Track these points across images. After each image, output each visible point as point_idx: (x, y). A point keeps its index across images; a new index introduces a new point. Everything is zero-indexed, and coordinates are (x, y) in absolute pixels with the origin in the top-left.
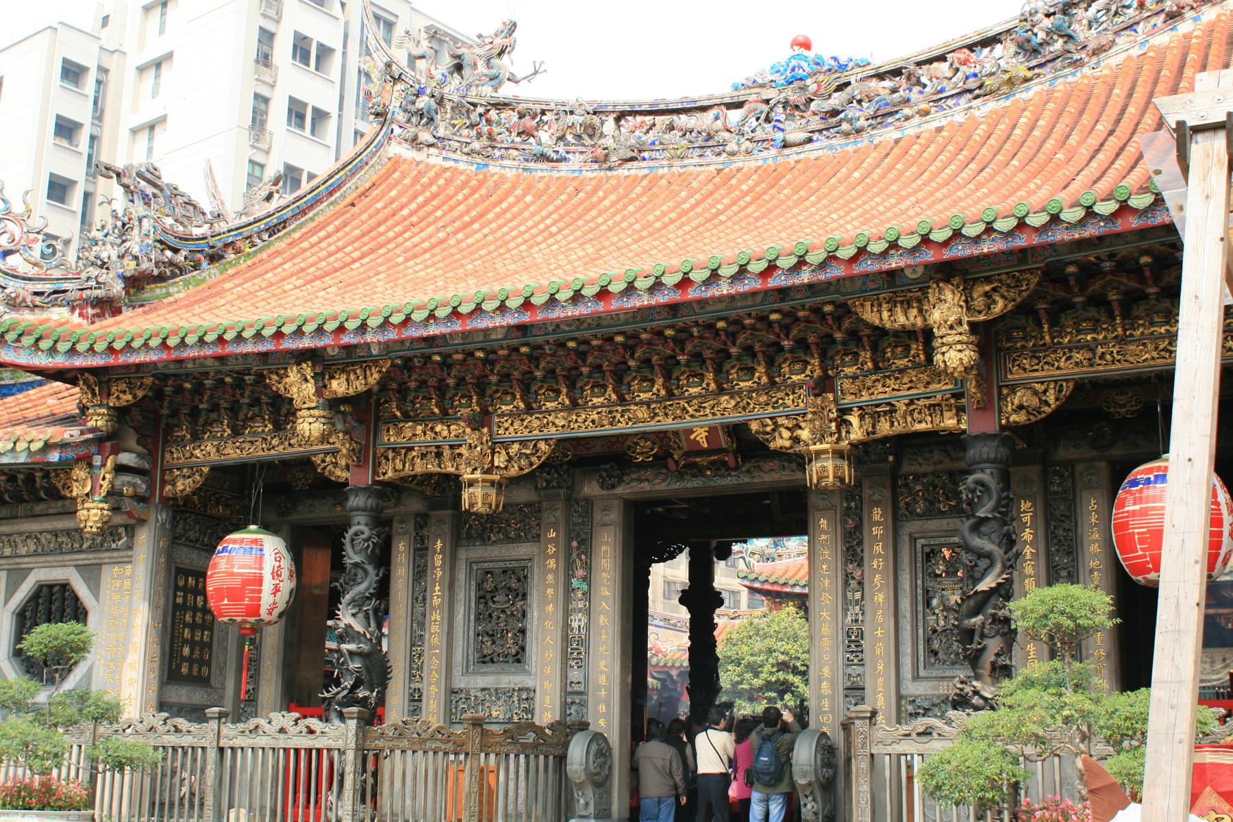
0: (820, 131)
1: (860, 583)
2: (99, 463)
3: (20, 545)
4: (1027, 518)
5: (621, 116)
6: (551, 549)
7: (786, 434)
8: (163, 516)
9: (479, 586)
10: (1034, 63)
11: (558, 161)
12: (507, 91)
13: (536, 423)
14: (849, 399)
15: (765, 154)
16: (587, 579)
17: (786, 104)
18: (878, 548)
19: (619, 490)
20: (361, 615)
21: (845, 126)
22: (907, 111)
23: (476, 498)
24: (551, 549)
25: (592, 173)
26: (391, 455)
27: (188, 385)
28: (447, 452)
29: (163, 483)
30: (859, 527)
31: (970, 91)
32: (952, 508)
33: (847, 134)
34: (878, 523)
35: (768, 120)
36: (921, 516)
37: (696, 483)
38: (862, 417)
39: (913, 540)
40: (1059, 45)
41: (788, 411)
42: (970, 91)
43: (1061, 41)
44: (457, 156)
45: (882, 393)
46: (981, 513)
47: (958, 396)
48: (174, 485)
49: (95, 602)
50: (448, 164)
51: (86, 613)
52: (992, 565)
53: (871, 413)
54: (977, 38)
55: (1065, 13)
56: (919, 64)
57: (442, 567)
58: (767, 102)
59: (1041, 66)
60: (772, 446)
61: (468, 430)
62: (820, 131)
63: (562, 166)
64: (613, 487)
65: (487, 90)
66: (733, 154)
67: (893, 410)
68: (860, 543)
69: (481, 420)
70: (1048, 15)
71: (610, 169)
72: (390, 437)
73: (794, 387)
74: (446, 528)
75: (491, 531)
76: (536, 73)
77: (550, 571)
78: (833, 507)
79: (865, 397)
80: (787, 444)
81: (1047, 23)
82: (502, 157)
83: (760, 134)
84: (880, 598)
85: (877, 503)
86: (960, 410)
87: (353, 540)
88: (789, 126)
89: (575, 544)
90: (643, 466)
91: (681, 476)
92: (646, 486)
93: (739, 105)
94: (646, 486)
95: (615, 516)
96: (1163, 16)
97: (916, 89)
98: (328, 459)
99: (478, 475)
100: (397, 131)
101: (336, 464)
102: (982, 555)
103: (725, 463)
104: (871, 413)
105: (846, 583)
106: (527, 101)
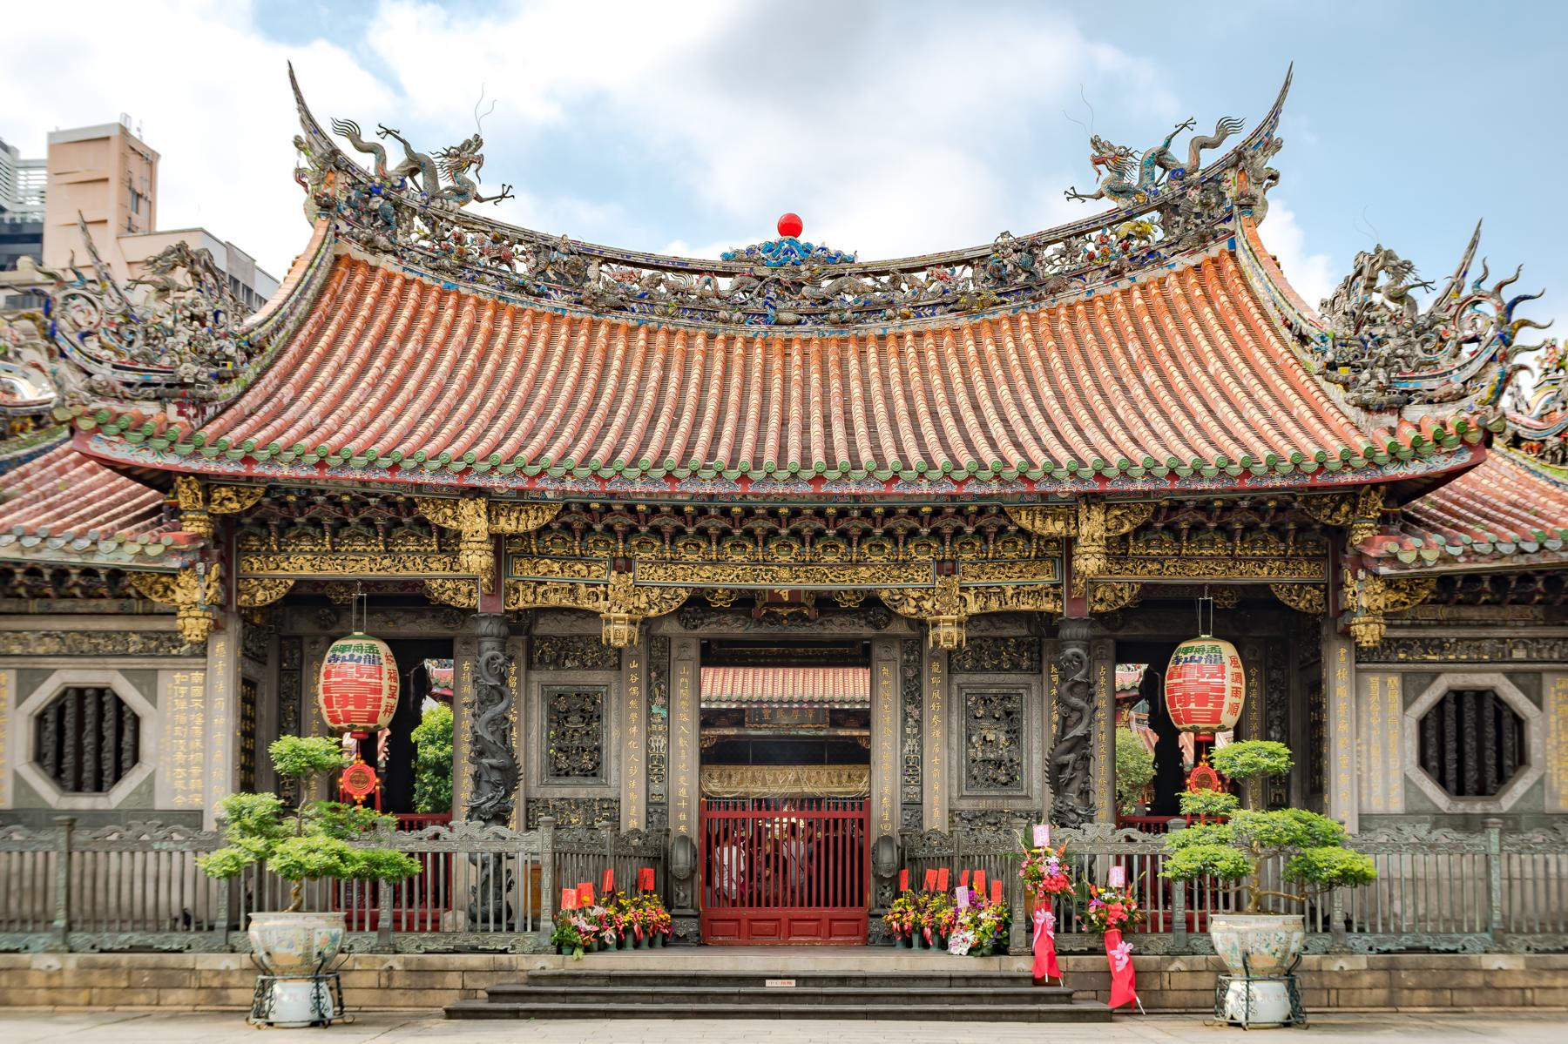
0: (809, 315)
1: (919, 723)
2: (202, 572)
3: (33, 644)
4: (1056, 678)
5: (607, 261)
6: (634, 679)
7: (913, 603)
8: (239, 626)
9: (551, 708)
10: (1001, 290)
11: (540, 295)
12: (472, 208)
13: (680, 573)
14: (969, 581)
15: (755, 327)
16: (667, 706)
17: (777, 281)
18: (936, 695)
19: (698, 631)
20: (498, 734)
21: (833, 316)
22: (890, 312)
23: (619, 633)
24: (634, 679)
25: (583, 314)
26: (521, 587)
27: (292, 498)
28: (582, 589)
29: (239, 591)
30: (918, 676)
31: (945, 304)
32: (994, 666)
33: (834, 323)
34: (936, 675)
35: (759, 294)
36: (969, 671)
37: (775, 630)
38: (977, 596)
39: (960, 688)
40: (1022, 278)
41: (917, 585)
42: (945, 304)
43: (1024, 276)
44: (421, 269)
45: (996, 579)
46: (1077, 677)
47: (1055, 586)
48: (253, 596)
49: (150, 707)
50: (409, 276)
51: (136, 720)
52: (1081, 719)
53: (984, 593)
54: (954, 258)
55: (1030, 252)
56: (903, 271)
57: (518, 688)
58: (761, 279)
59: (1006, 294)
60: (899, 611)
61: (614, 573)
62: (809, 315)
63: (544, 301)
64: (696, 627)
65: (452, 204)
66: (724, 321)
67: (1003, 591)
68: (919, 689)
69: (624, 565)
70: (1016, 251)
71: (597, 314)
72: (525, 570)
73: (920, 564)
74: (521, 654)
75: (566, 657)
76: (503, 196)
77: (634, 697)
78: (894, 660)
79: (984, 581)
80: (913, 611)
81: (1015, 257)
82: (473, 279)
83: (751, 307)
84: (937, 733)
85: (936, 659)
86: (1057, 597)
87: (488, 663)
88: (780, 305)
89: (654, 674)
90: (721, 611)
91: (760, 622)
92: (725, 629)
93: (731, 275)
94: (725, 629)
95: (694, 652)
96: (1106, 272)
97: (897, 293)
98: (449, 585)
99: (622, 614)
100: (344, 228)
101: (457, 590)
102: (1074, 709)
103: (800, 615)
104: (984, 593)
105: (905, 720)
106: (502, 226)
